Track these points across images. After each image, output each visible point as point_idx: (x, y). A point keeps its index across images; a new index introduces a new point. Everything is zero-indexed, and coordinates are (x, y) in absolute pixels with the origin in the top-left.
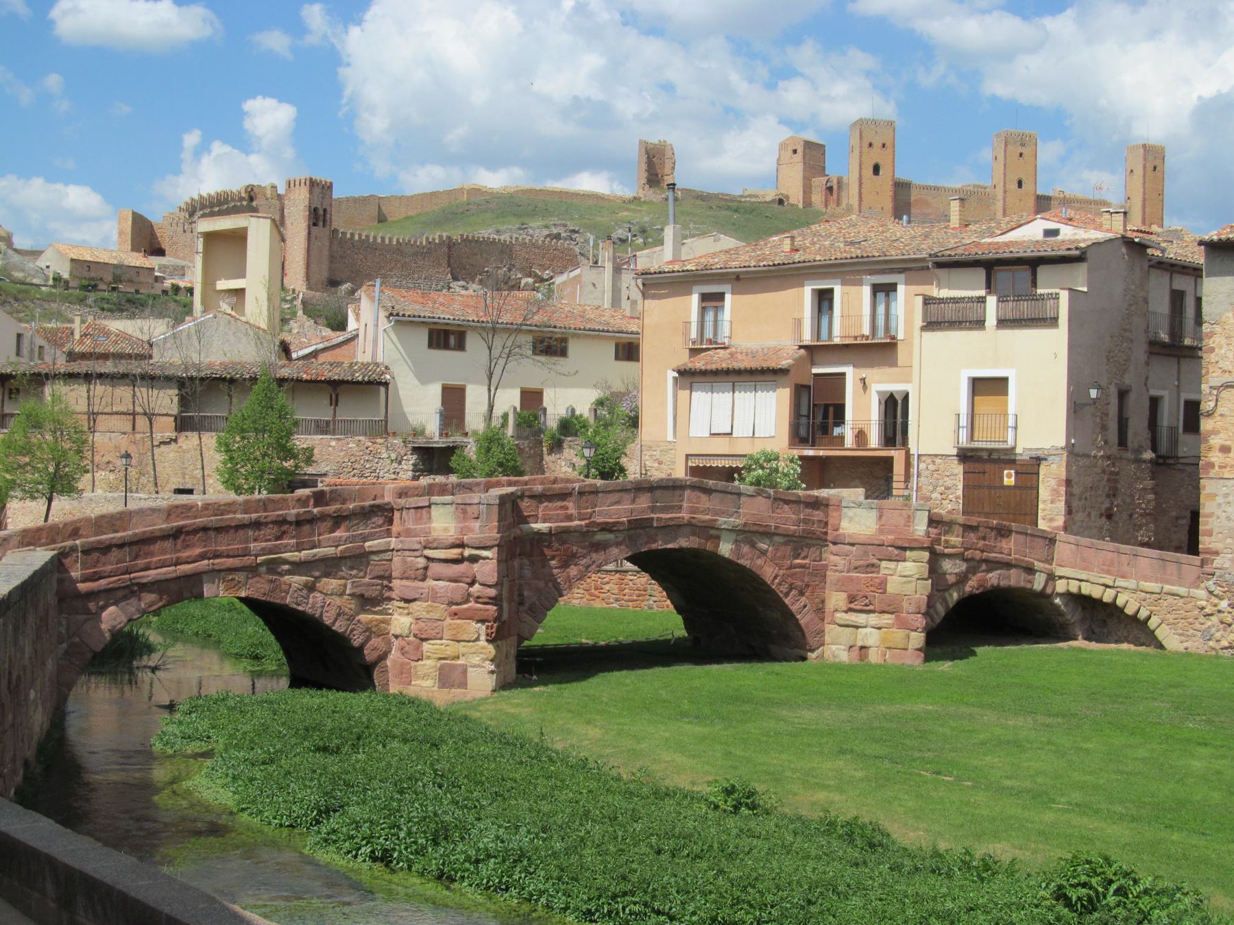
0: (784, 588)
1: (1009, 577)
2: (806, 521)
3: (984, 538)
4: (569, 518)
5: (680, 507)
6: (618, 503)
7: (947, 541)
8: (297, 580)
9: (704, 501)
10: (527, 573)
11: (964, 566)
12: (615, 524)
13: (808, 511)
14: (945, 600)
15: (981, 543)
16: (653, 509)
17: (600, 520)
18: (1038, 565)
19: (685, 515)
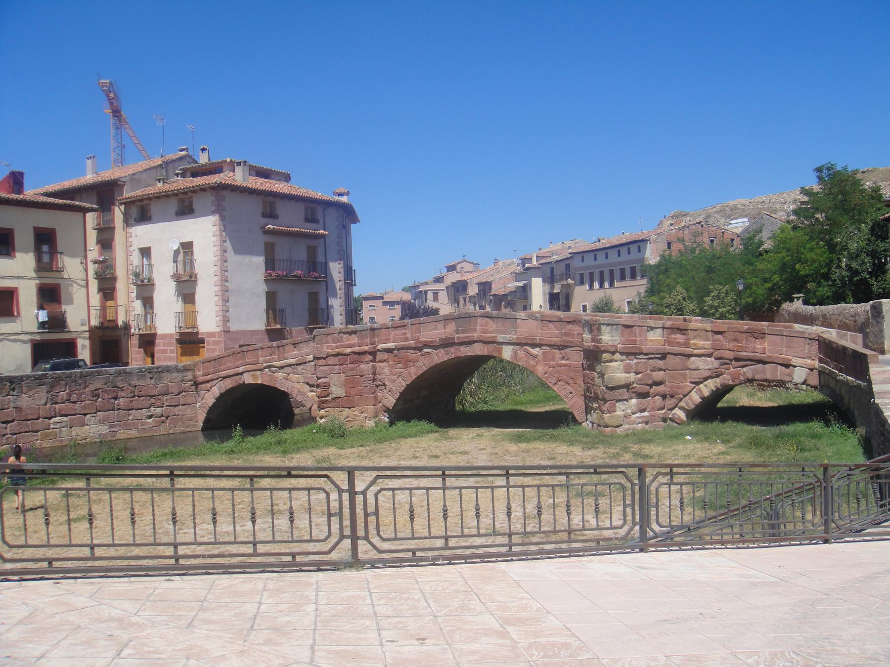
0: (554, 380)
1: (764, 372)
2: (565, 334)
3: (735, 340)
4: (407, 339)
5: (475, 330)
6: (436, 329)
7: (695, 344)
8: (280, 375)
9: (492, 325)
10: (386, 370)
11: (716, 364)
12: (431, 342)
13: (570, 326)
14: (700, 390)
15: (732, 345)
16: (457, 332)
17: (422, 339)
18: (795, 361)
19: (476, 335)
